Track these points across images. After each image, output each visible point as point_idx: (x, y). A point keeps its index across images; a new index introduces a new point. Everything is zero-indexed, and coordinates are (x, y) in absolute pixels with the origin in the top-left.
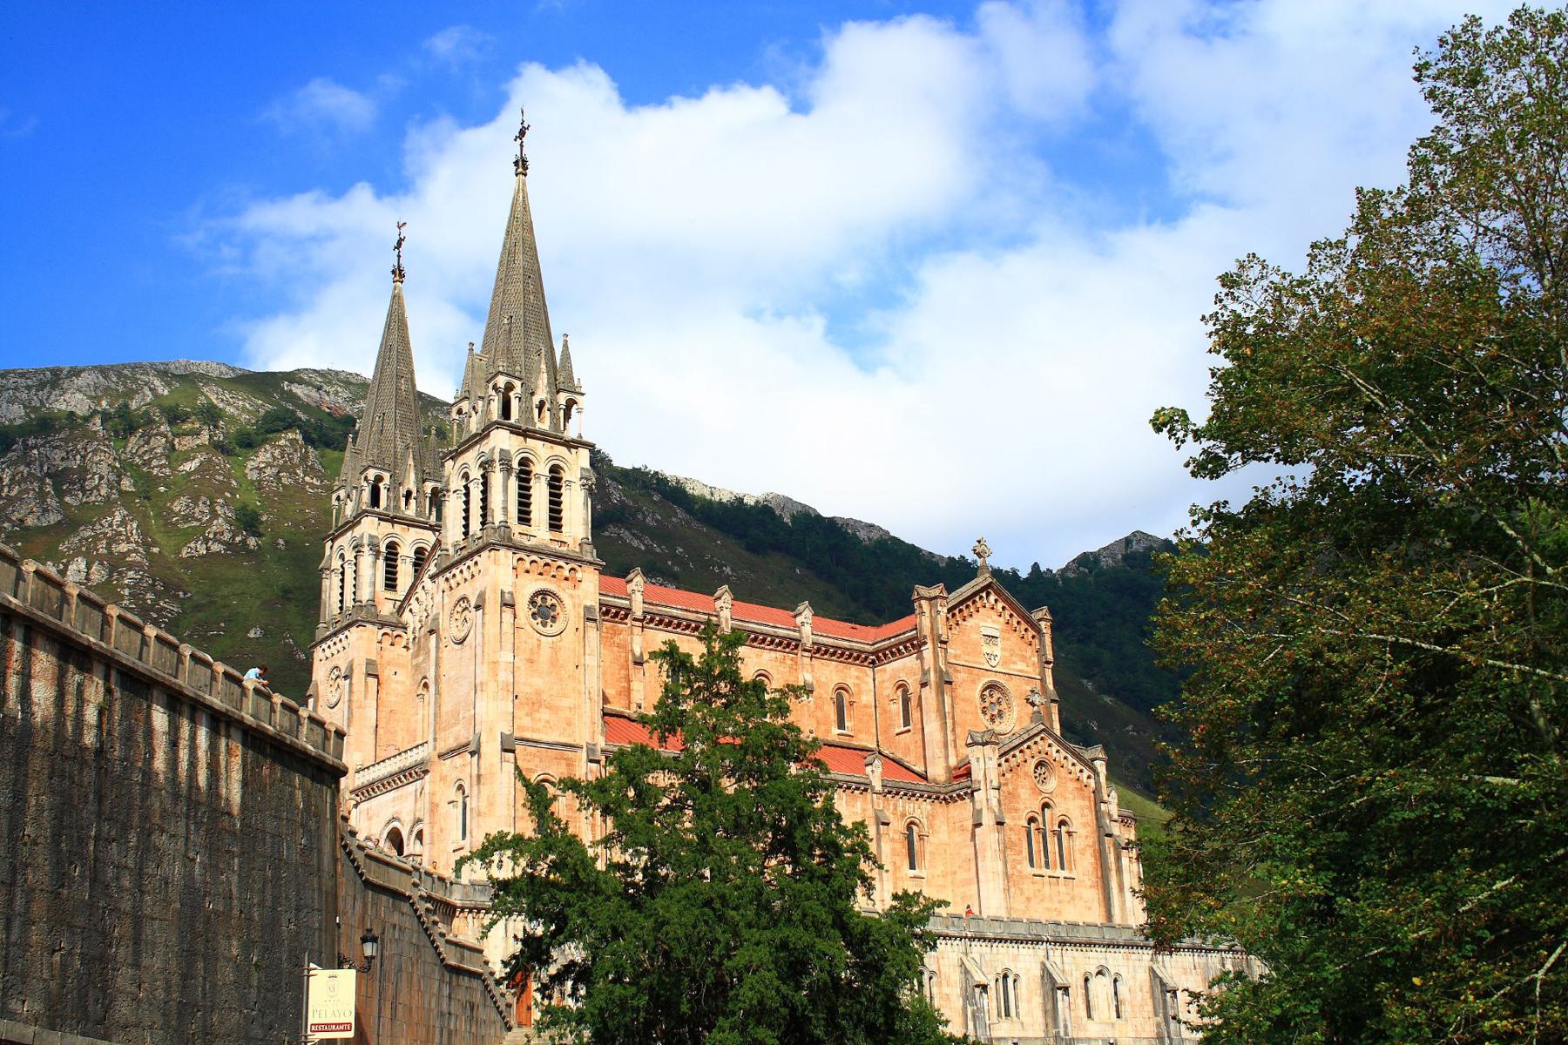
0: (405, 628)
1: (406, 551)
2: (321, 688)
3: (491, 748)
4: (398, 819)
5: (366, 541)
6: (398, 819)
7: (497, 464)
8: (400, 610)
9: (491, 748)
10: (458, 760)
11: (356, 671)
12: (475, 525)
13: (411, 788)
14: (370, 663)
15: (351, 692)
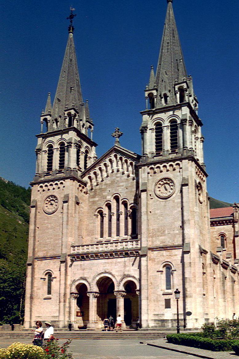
0: (85, 184)
1: (83, 150)
2: (38, 203)
3: (194, 251)
4: (110, 274)
5: (73, 141)
6: (110, 274)
7: (188, 122)
8: (83, 175)
9: (194, 251)
10: (164, 253)
11: (70, 199)
12: (167, 145)
13: (119, 260)
14: (76, 197)
15: (68, 209)
